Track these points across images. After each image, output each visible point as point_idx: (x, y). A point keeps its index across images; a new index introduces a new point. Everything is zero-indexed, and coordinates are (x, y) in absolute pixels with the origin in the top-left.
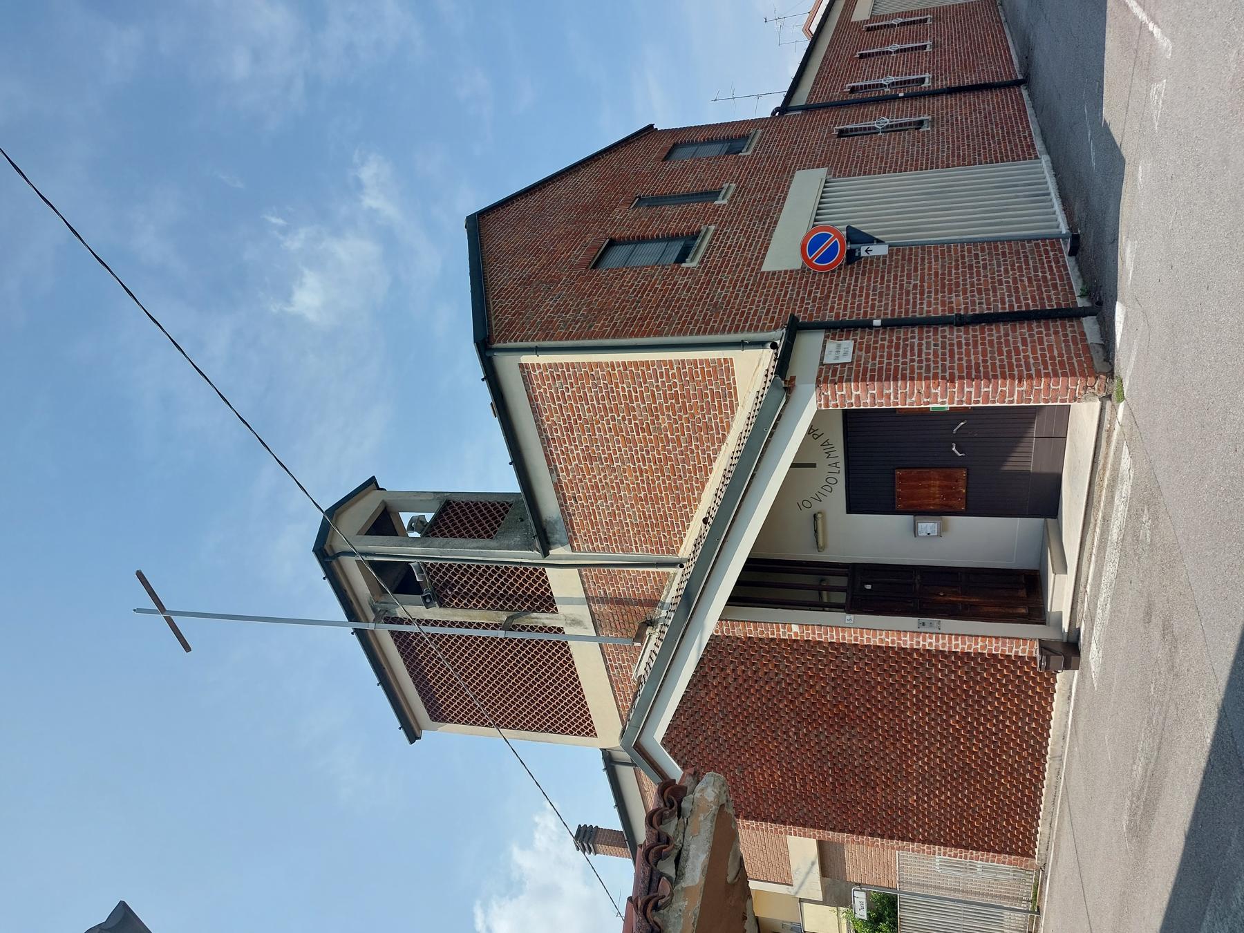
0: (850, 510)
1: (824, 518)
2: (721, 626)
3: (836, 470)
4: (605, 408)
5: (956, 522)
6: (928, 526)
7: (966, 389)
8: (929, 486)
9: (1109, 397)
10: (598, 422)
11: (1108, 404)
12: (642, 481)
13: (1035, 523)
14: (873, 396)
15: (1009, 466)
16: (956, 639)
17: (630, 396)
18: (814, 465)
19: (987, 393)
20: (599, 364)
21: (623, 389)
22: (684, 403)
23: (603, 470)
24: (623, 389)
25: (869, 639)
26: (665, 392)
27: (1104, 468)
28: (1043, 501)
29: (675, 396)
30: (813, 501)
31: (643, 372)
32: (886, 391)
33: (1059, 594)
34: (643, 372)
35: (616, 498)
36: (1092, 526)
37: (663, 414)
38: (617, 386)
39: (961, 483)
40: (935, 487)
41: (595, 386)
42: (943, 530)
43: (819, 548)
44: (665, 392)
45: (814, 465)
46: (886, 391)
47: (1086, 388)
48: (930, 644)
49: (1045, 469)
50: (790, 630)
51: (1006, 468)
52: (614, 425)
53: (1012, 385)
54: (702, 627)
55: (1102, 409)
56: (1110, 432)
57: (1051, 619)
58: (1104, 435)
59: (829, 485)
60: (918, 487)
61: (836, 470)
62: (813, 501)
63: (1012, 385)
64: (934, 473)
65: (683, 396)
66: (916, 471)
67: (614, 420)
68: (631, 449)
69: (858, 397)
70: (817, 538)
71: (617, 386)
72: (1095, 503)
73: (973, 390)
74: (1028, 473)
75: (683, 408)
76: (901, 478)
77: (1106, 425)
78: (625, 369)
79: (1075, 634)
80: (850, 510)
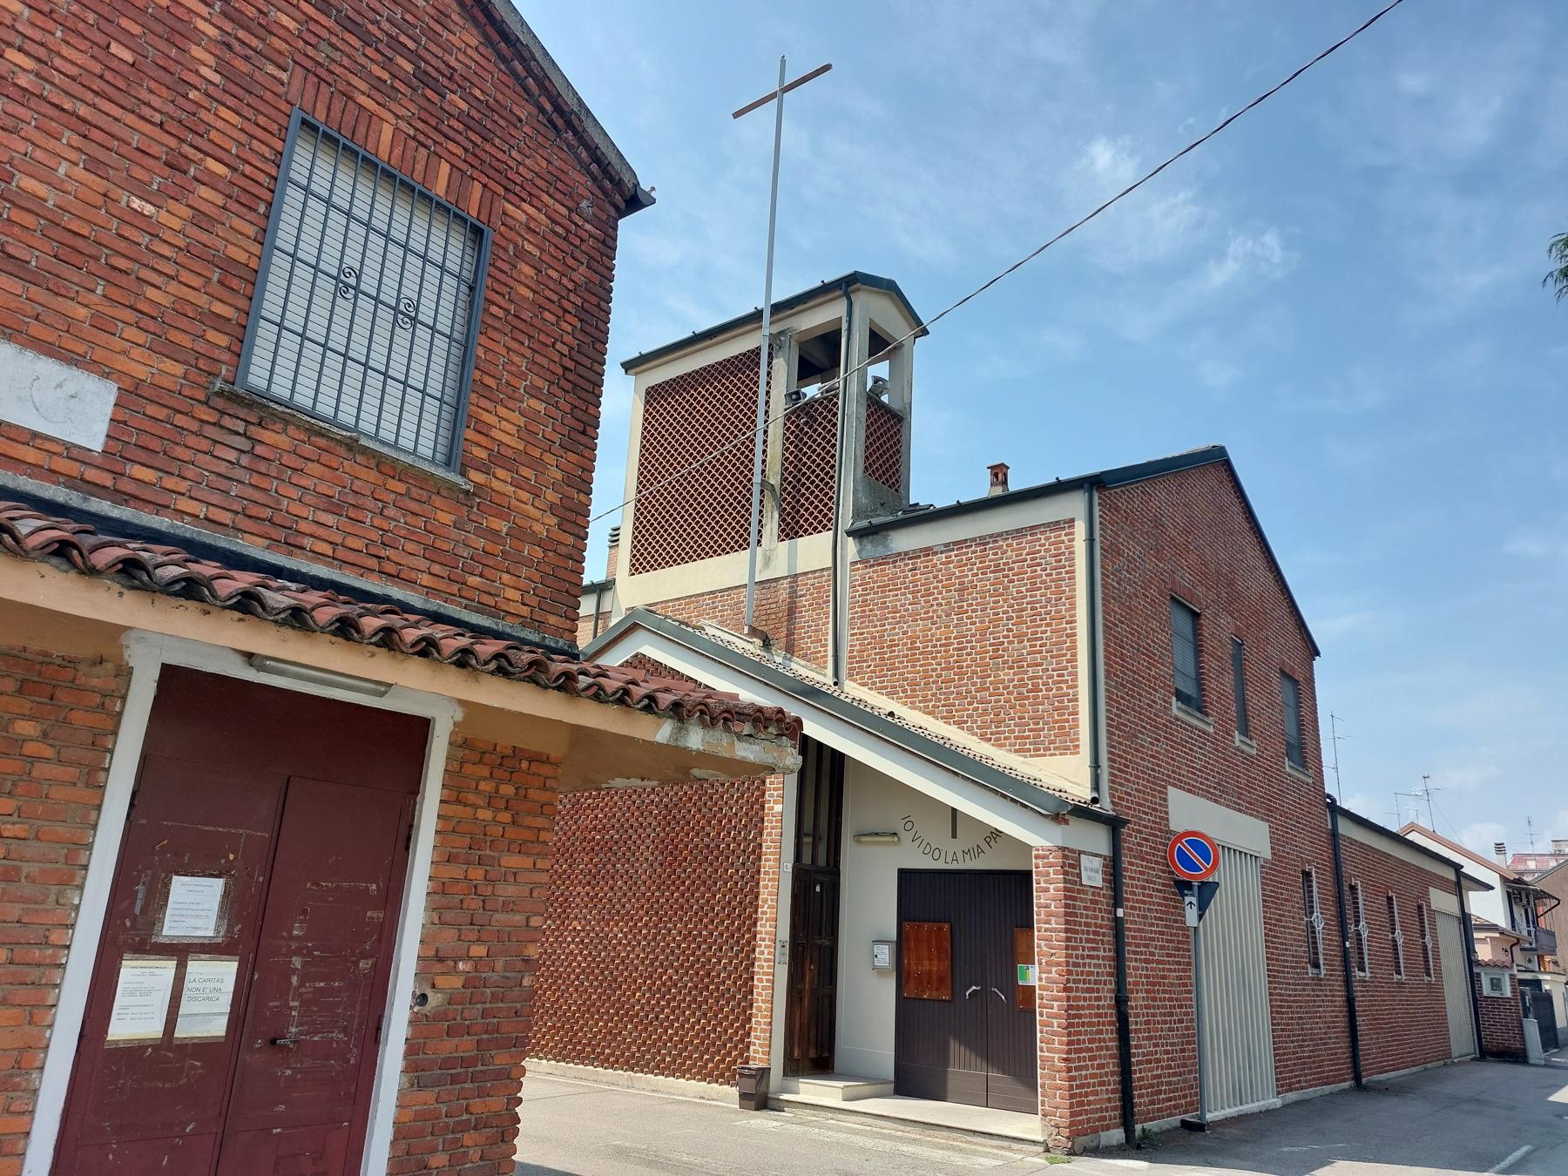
3: (949, 859)
6: (885, 955)
7: (1055, 1004)
9: (1047, 1150)
10: (1005, 601)
11: (1041, 1149)
13: (889, 1069)
14: (1047, 906)
15: (954, 1046)
18: (954, 836)
20: (1073, 607)
21: (1044, 632)
23: (949, 603)
24: (1044, 632)
25: (766, 887)
28: (914, 1078)
29: (1036, 689)
33: (812, 1090)
40: (929, 965)
41: (1049, 601)
42: (880, 971)
43: (859, 836)
45: (954, 836)
49: (951, 1084)
50: (776, 802)
53: (1061, 1052)
55: (1034, 1142)
56: (1009, 1149)
57: (791, 1082)
58: (1006, 1144)
59: (931, 851)
63: (1061, 1052)
66: (948, 946)
69: (1047, 890)
74: (946, 1064)
75: (1021, 697)
76: (940, 929)
77: (1015, 1146)
78: (1068, 636)
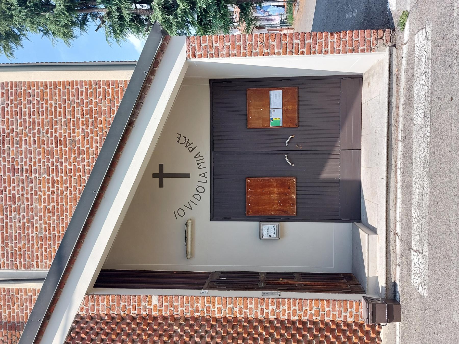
0: (214, 218)
1: (193, 224)
2: (87, 302)
3: (204, 179)
4: (34, 122)
5: (291, 227)
6: (270, 229)
7: (295, 41)
8: (270, 193)
9: (394, 46)
10: (26, 135)
11: (394, 49)
12: (53, 192)
13: (345, 227)
14: (228, 48)
15: (326, 175)
16: (294, 305)
17: (56, 111)
18: (188, 176)
19: (309, 45)
20: (35, 84)
21: (51, 105)
22: (96, 118)
23: (23, 181)
24: (51, 105)
25: (220, 310)
26: (82, 108)
27: (397, 107)
28: (351, 210)
29: (90, 112)
30: (186, 209)
31: (68, 90)
32: (238, 43)
33: (375, 270)
34: (68, 90)
35: (29, 210)
36: (393, 167)
37: (79, 128)
38: (46, 103)
39: (293, 190)
40: (274, 193)
41: (30, 102)
42: (281, 234)
43: (187, 255)
44: (82, 108)
45: (188, 176)
46: (238, 43)
47: (377, 39)
48: (273, 311)
49: (349, 177)
50: (150, 303)
51: (322, 177)
52: (39, 138)
53: (327, 36)
54: (70, 304)
55: (391, 55)
56: (398, 75)
57: (370, 286)
58: (394, 78)
59: (198, 195)
60: (263, 194)
61: (204, 179)
62: (186, 209)
63: (327, 36)
64: (273, 182)
65: (96, 113)
66: (260, 180)
67: (39, 132)
68: (48, 161)
69: (217, 48)
70: (186, 246)
71: (46, 103)
72: (394, 145)
73: (299, 42)
74: (337, 182)
75: (95, 123)
76: (250, 186)
77: (395, 70)
78: (55, 88)
79: (392, 288)
80: (214, 218)
